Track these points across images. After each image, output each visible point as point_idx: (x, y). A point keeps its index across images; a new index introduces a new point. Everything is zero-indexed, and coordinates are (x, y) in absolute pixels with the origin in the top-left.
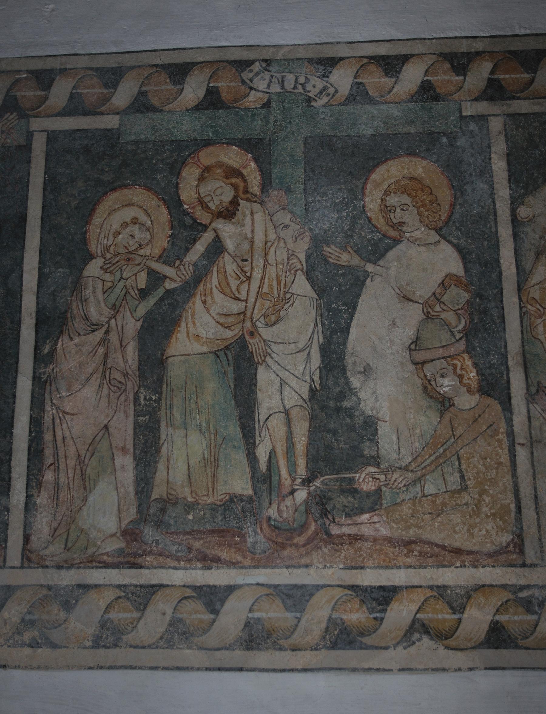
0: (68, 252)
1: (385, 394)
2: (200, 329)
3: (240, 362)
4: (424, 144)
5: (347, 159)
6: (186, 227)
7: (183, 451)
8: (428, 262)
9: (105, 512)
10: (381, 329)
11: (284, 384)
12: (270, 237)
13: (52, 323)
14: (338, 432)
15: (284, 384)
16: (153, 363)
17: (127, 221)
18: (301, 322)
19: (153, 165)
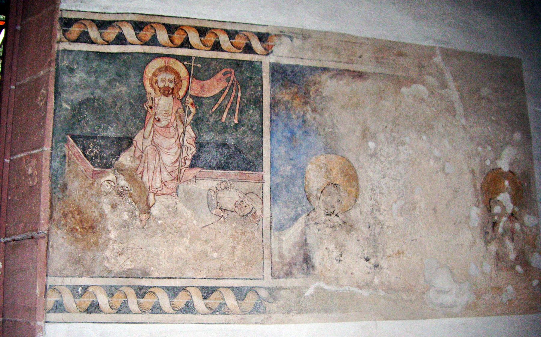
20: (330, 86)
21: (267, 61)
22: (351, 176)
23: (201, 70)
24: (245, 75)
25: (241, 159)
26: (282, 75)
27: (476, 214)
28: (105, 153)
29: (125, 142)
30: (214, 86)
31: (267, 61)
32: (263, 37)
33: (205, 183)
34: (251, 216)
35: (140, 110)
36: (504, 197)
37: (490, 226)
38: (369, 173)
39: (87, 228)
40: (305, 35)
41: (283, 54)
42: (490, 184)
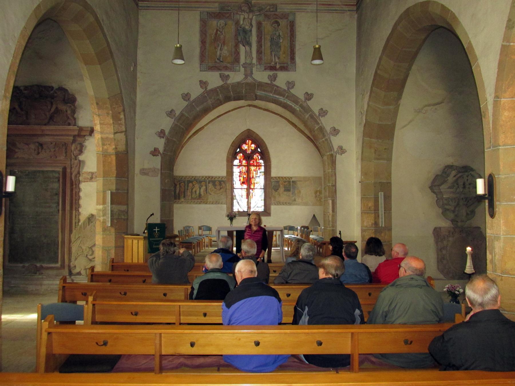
0: (188, 186)
1: (202, 193)
2: (194, 190)
3: (196, 192)
4: (204, 181)
5: (200, 182)
6: (193, 185)
7: (193, 196)
8: (204, 187)
9: (190, 198)
10: (202, 190)
11: (198, 192)
12: (197, 186)
13: (187, 189)
14: (200, 195)
15: (198, 192)
16: (192, 192)
17: (190, 184)
18: (199, 189)
19: (192, 182)
20: (298, 183)
21: (291, 180)
22: (300, 192)
24: (289, 182)
25: (289, 190)
26: (293, 182)
27: (314, 195)
28: (276, 190)
29: (278, 189)
31: (291, 180)
33: (285, 193)
34: (289, 196)
35: (279, 185)
36: (318, 193)
37: (316, 197)
39: (275, 197)
40: (295, 177)
41: (293, 179)
42: (316, 192)
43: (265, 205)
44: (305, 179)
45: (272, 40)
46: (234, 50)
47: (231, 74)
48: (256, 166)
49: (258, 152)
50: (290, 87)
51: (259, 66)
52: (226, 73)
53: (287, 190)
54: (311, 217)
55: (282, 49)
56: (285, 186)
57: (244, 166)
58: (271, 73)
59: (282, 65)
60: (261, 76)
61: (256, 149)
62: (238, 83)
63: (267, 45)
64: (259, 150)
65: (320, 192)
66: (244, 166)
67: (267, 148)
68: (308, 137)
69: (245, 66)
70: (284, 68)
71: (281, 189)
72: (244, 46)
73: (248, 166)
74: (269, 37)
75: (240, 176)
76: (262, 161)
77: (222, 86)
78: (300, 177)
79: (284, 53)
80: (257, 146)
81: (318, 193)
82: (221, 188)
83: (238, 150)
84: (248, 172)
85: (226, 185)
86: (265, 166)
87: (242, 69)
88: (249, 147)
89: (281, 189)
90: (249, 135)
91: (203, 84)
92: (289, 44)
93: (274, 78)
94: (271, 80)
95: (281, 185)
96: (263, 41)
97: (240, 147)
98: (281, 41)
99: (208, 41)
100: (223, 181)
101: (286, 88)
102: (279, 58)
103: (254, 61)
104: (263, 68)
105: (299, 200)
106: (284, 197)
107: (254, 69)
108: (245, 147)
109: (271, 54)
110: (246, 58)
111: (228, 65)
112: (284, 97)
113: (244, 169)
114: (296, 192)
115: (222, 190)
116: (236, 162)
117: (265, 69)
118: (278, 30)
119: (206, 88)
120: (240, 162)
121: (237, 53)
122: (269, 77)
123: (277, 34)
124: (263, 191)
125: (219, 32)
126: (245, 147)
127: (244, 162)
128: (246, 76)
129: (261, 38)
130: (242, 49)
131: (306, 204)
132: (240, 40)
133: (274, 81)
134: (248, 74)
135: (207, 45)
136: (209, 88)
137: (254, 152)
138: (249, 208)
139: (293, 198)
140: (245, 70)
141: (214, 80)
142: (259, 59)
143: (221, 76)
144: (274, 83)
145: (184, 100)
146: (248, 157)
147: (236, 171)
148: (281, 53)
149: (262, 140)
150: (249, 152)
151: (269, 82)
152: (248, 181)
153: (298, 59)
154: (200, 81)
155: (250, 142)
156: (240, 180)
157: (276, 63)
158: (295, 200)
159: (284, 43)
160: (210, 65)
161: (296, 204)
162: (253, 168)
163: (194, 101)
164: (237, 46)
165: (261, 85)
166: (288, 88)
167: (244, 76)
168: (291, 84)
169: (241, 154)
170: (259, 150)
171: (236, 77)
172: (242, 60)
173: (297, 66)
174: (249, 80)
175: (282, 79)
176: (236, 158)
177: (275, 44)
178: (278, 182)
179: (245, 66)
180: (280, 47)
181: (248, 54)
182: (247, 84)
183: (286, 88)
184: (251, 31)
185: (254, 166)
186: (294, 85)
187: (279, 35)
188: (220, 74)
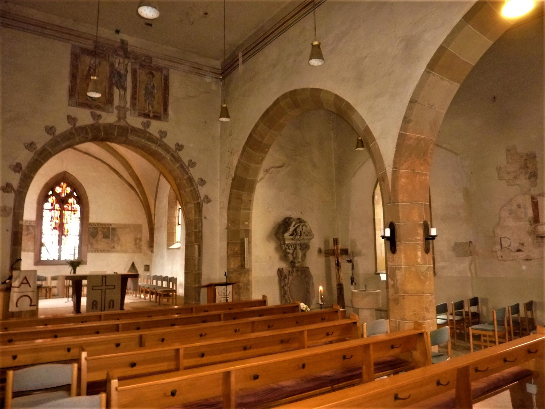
20: (118, 230)
23: (104, 228)
24: (108, 229)
26: (113, 229)
27: (134, 243)
29: (96, 236)
30: (105, 230)
31: (111, 227)
32: (111, 225)
33: (104, 240)
35: (97, 233)
37: (136, 244)
38: (122, 238)
40: (115, 224)
41: (113, 226)
42: (136, 240)
43: (80, 253)
44: (124, 227)
45: (147, 88)
46: (107, 91)
47: (104, 114)
48: (71, 211)
49: (74, 197)
50: (163, 136)
51: (133, 111)
52: (98, 112)
53: (106, 236)
54: (131, 264)
55: (156, 99)
56: (104, 233)
57: (57, 210)
58: (145, 120)
59: (156, 114)
60: (135, 121)
61: (71, 193)
62: (111, 125)
63: (141, 93)
64: (75, 194)
65: (140, 240)
66: (57, 210)
67: (85, 192)
68: (130, 186)
69: (119, 108)
70: (157, 117)
71: (100, 236)
72: (118, 88)
73: (62, 210)
74: (143, 86)
75: (51, 221)
76: (77, 207)
77: (92, 125)
78: (120, 224)
79: (158, 103)
80: (74, 190)
81: (137, 241)
82: (28, 234)
83: (50, 193)
84: (62, 216)
85: (35, 230)
86: (82, 212)
87: (116, 112)
88: (62, 190)
89: (100, 236)
90: (63, 178)
91: (71, 119)
92: (163, 96)
93: (148, 125)
94: (145, 127)
95: (100, 232)
96: (138, 88)
97: (53, 190)
98: (155, 91)
99: (79, 75)
100: (31, 226)
101: (159, 137)
102: (152, 107)
103: (128, 105)
104: (137, 114)
105: (118, 248)
106: (102, 244)
107: (128, 113)
108: (58, 190)
109: (146, 102)
110: (119, 101)
111: (101, 105)
112: (156, 144)
113: (57, 214)
114: (115, 239)
115: (30, 236)
116: (47, 206)
117: (139, 115)
118: (152, 81)
119: (75, 125)
120: (52, 205)
121: (111, 95)
122: (143, 124)
123: (152, 84)
124: (78, 237)
125: (92, 70)
126: (58, 190)
127: (57, 206)
128: (119, 119)
129: (136, 85)
130: (117, 92)
131: (125, 252)
132: (114, 81)
133: (148, 128)
134: (122, 117)
135: (78, 80)
136: (78, 125)
137: (69, 196)
138: (60, 256)
139: (112, 245)
140: (119, 113)
141: (84, 117)
142: (134, 105)
143: (92, 114)
144: (148, 130)
145: (48, 133)
146: (62, 201)
147: (47, 215)
148: (155, 102)
149: (81, 184)
150: (63, 195)
151: (143, 129)
152: (60, 228)
153: (170, 112)
154: (68, 116)
155: (65, 185)
156: (51, 225)
157: (149, 111)
158: (114, 247)
159: (158, 94)
160: (80, 100)
161: (115, 252)
162: (66, 213)
163: (60, 136)
164: (111, 87)
165: (134, 130)
166: (161, 137)
167: (117, 119)
168: (163, 134)
169: (54, 198)
170: (75, 194)
171: (109, 118)
172: (116, 102)
173: (169, 117)
174: (122, 123)
175: (155, 127)
176: (47, 201)
177: (149, 93)
178: (96, 228)
179: (119, 108)
180: (154, 97)
181: (123, 98)
182: (120, 127)
183: (159, 137)
184: (126, 76)
185: (68, 210)
186: (166, 135)
187: (154, 86)
188: (92, 113)
